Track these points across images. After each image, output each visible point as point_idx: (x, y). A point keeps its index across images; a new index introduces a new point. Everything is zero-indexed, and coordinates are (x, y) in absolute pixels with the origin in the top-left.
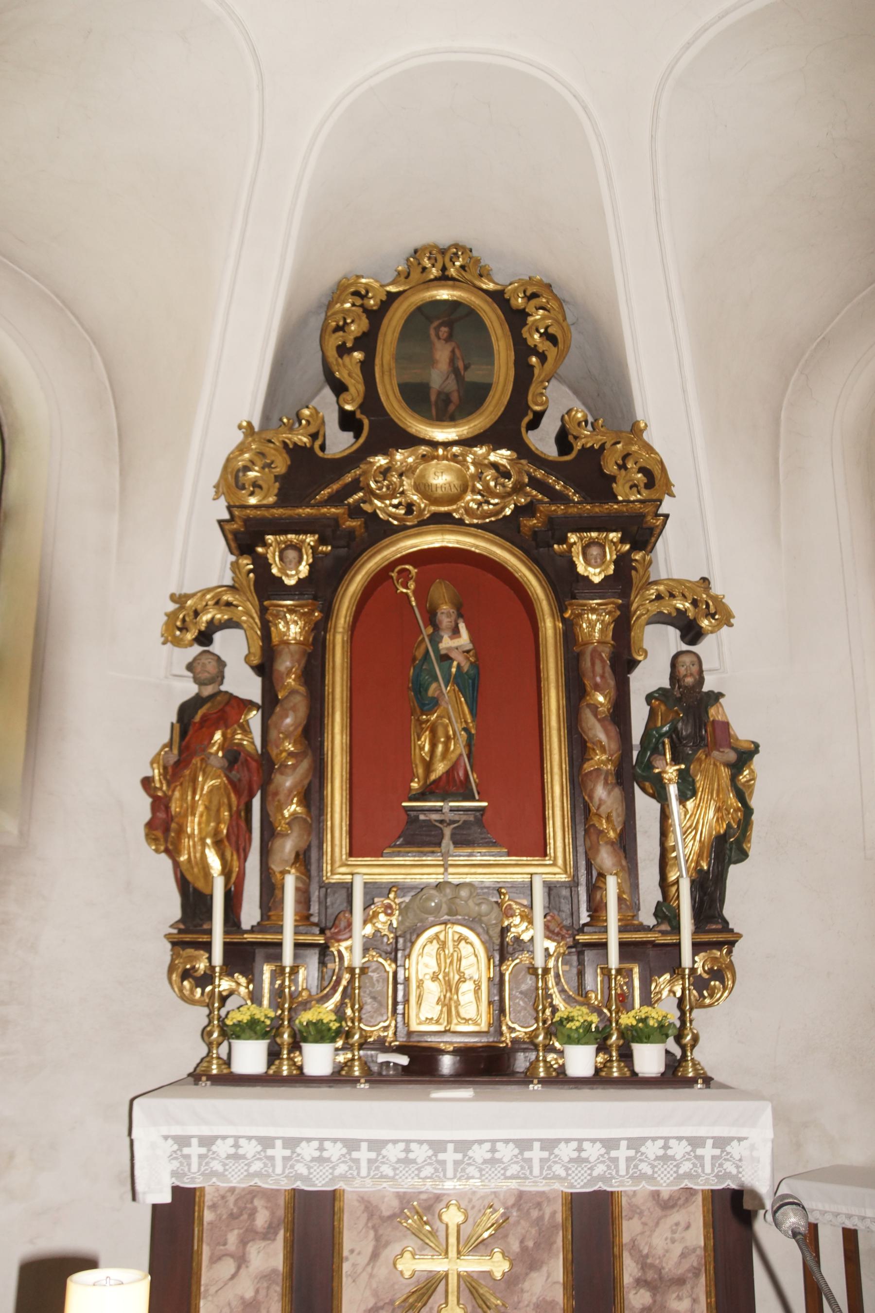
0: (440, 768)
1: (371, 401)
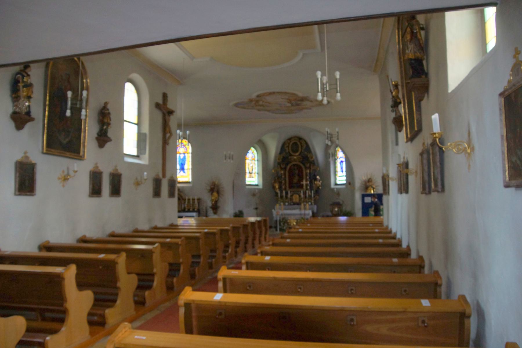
1: (289, 152)
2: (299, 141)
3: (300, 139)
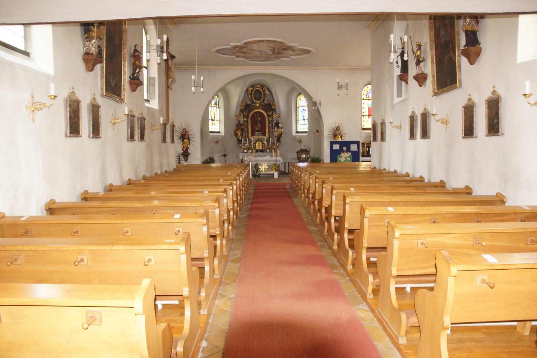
1: (252, 99)
2: (262, 89)
3: (262, 86)
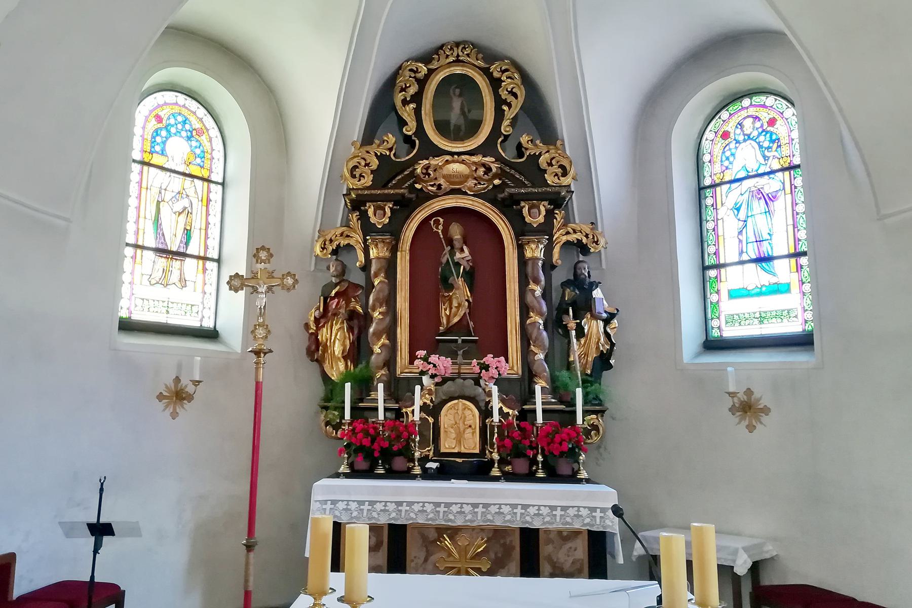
0: (456, 320)
2: (486, 72)
3: (490, 56)
